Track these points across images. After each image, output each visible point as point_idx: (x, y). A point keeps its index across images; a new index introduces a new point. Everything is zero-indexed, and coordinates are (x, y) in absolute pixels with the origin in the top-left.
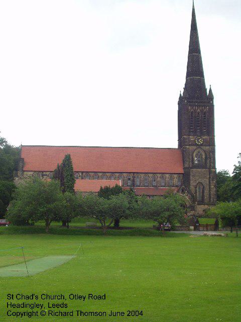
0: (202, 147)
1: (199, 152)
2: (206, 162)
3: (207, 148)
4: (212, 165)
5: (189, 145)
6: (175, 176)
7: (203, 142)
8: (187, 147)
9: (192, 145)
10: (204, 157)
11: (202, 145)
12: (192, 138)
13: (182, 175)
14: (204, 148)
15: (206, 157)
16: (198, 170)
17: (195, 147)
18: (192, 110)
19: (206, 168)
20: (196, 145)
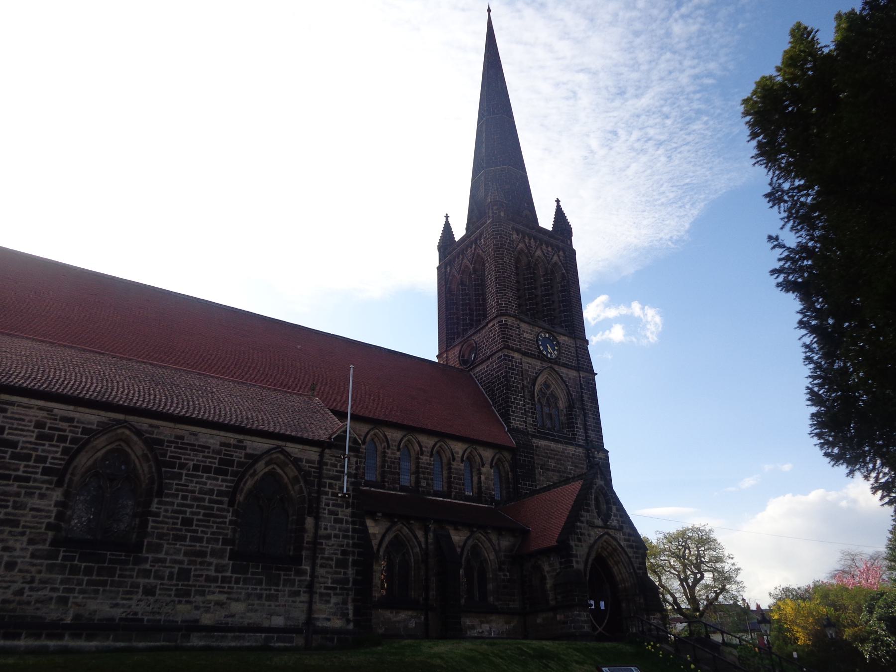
0: (556, 367)
1: (547, 385)
2: (571, 425)
3: (573, 374)
4: (592, 434)
5: (525, 354)
6: (487, 454)
7: (559, 351)
8: (517, 355)
9: (532, 356)
10: (562, 404)
11: (556, 362)
12: (528, 332)
13: (507, 455)
14: (563, 371)
15: (571, 407)
16: (553, 445)
17: (538, 364)
18: (521, 245)
19: (571, 440)
20: (542, 357)
